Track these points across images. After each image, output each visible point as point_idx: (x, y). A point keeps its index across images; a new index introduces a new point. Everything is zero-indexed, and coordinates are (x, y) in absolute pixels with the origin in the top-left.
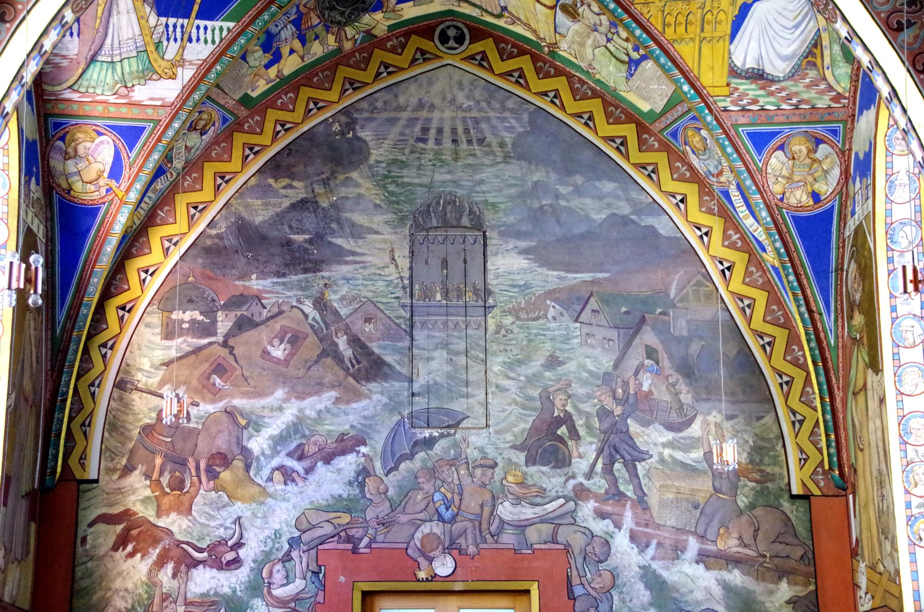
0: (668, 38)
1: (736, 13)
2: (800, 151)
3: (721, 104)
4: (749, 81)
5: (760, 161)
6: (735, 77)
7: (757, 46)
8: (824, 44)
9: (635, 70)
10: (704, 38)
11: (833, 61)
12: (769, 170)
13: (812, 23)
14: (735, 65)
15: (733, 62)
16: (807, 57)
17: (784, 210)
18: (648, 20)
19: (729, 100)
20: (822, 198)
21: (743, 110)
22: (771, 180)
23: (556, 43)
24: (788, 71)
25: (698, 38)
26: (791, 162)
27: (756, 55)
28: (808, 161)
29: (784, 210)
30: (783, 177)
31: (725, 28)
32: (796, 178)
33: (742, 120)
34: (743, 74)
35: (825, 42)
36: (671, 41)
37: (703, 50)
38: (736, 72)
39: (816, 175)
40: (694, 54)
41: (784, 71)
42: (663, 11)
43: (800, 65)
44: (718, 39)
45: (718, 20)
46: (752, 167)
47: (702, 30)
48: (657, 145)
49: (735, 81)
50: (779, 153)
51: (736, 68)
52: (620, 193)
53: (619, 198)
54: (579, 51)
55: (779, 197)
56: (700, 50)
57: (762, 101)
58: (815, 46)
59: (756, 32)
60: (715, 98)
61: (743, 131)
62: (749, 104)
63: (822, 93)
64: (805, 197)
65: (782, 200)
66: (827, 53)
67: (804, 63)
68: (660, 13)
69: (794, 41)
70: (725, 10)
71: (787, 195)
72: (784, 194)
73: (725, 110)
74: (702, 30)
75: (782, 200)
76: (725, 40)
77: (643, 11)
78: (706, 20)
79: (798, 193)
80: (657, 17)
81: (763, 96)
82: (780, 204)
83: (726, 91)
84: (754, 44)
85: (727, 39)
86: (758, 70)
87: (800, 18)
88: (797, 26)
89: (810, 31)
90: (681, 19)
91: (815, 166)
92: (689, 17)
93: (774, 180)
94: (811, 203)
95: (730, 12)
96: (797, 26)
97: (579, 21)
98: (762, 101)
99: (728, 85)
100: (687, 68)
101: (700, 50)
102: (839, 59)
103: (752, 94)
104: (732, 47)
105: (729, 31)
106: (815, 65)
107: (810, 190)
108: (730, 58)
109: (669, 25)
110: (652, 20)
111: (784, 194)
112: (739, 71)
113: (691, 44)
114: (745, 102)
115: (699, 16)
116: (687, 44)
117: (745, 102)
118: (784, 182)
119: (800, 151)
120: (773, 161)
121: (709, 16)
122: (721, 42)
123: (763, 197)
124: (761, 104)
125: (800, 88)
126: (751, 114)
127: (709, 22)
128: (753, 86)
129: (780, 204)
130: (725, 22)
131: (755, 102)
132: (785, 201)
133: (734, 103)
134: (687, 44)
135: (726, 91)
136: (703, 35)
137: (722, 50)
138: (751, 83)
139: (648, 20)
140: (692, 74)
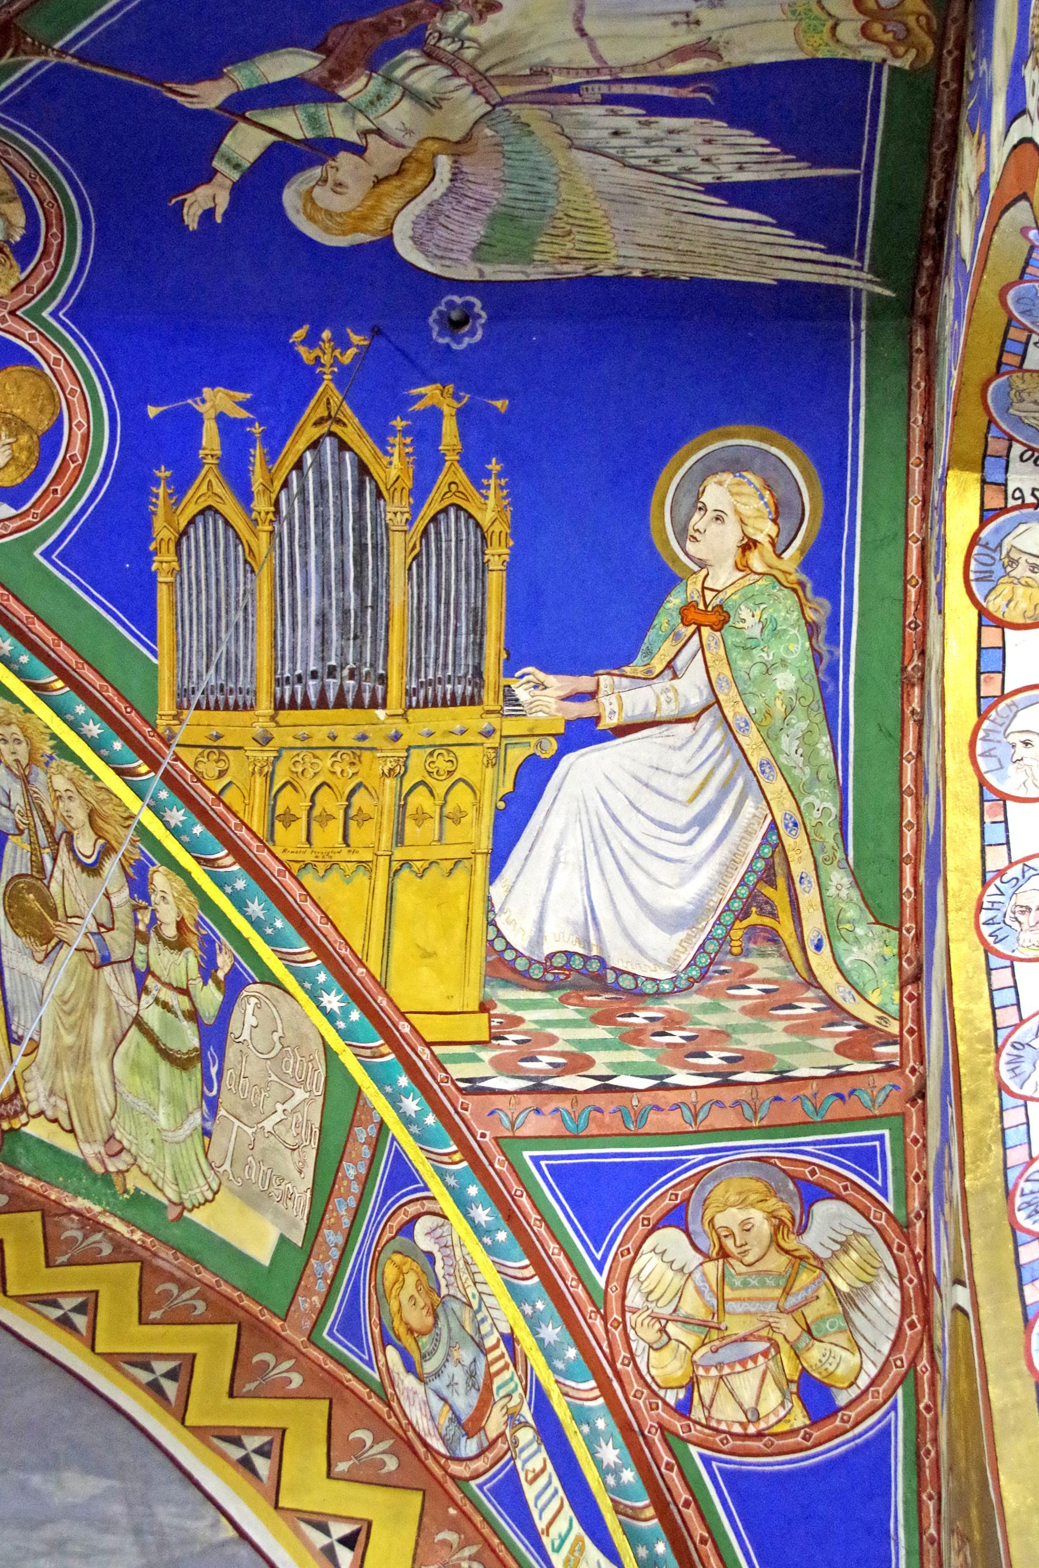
0: (283, 857)
1: (508, 787)
2: (746, 1227)
3: (457, 1071)
4: (556, 996)
5: (600, 1267)
6: (507, 983)
7: (578, 884)
8: (796, 869)
9: (220, 1074)
10: (406, 863)
11: (831, 922)
12: (634, 1299)
13: (749, 808)
14: (509, 946)
15: (499, 934)
16: (745, 914)
17: (694, 1450)
18: (218, 797)
19: (486, 1055)
20: (842, 1399)
21: (537, 1089)
22: (643, 1333)
23: (17, 1091)
24: (685, 959)
25: (383, 862)
26: (712, 1269)
27: (577, 913)
28: (777, 1262)
29: (694, 1450)
30: (686, 1322)
31: (472, 836)
32: (736, 1326)
33: (532, 1126)
34: (537, 973)
35: (801, 865)
36: (295, 868)
37: (400, 897)
38: (511, 966)
39: (811, 1313)
40: (369, 911)
41: (673, 960)
42: (271, 777)
43: (723, 941)
44: (449, 865)
45: (447, 810)
46: (571, 1286)
47: (399, 838)
48: (297, 1380)
49: (506, 996)
50: (671, 1237)
51: (509, 955)
52: (117, 1509)
53: (107, 1525)
54: (78, 1089)
55: (671, 1398)
56: (390, 898)
57: (602, 1061)
58: (769, 877)
59: (573, 843)
60: (438, 1050)
61: (536, 1160)
62: (561, 1070)
63: (808, 1028)
64: (772, 1397)
65: (683, 1409)
66: (808, 897)
67: (736, 934)
68: (259, 780)
69: (697, 867)
70: (473, 779)
71: (706, 1388)
72: (692, 1385)
73: (475, 1088)
74: (399, 838)
75: (683, 1409)
76: (472, 872)
77: (201, 767)
78: (410, 809)
79: (746, 1384)
80: (251, 790)
81: (604, 1045)
82: (678, 1425)
83: (477, 1027)
84: (568, 881)
85: (481, 864)
86: (586, 959)
87: (709, 794)
88: (702, 821)
89: (749, 832)
90: (330, 803)
91: (805, 1277)
92: (356, 799)
93: (651, 1334)
94: (799, 1418)
95: (488, 786)
96: (702, 821)
97: (61, 942)
98: (602, 1061)
99: (484, 1007)
100: (345, 952)
101: (390, 898)
102: (851, 913)
103: (566, 1038)
104: (497, 891)
105: (486, 844)
106: (774, 938)
107: (791, 1370)
108: (492, 923)
109: (289, 818)
110: (227, 797)
111: (692, 1385)
112: (521, 964)
113: (361, 879)
114: (543, 1063)
115: (388, 799)
116: (347, 878)
117: (543, 1063)
118: (692, 1341)
119: (746, 1227)
120: (647, 1263)
121: (420, 799)
122: (460, 876)
123: (605, 1389)
124: (599, 1070)
125: (732, 1014)
126: (564, 1103)
127: (421, 817)
128: (570, 1013)
129: (678, 1425)
130: (472, 813)
131: (577, 1063)
132: (698, 1413)
133: (501, 1065)
134: (347, 878)
135: (477, 1027)
136: (399, 854)
137: (463, 900)
138: (564, 1001)
139: (218, 797)
140: (360, 971)
